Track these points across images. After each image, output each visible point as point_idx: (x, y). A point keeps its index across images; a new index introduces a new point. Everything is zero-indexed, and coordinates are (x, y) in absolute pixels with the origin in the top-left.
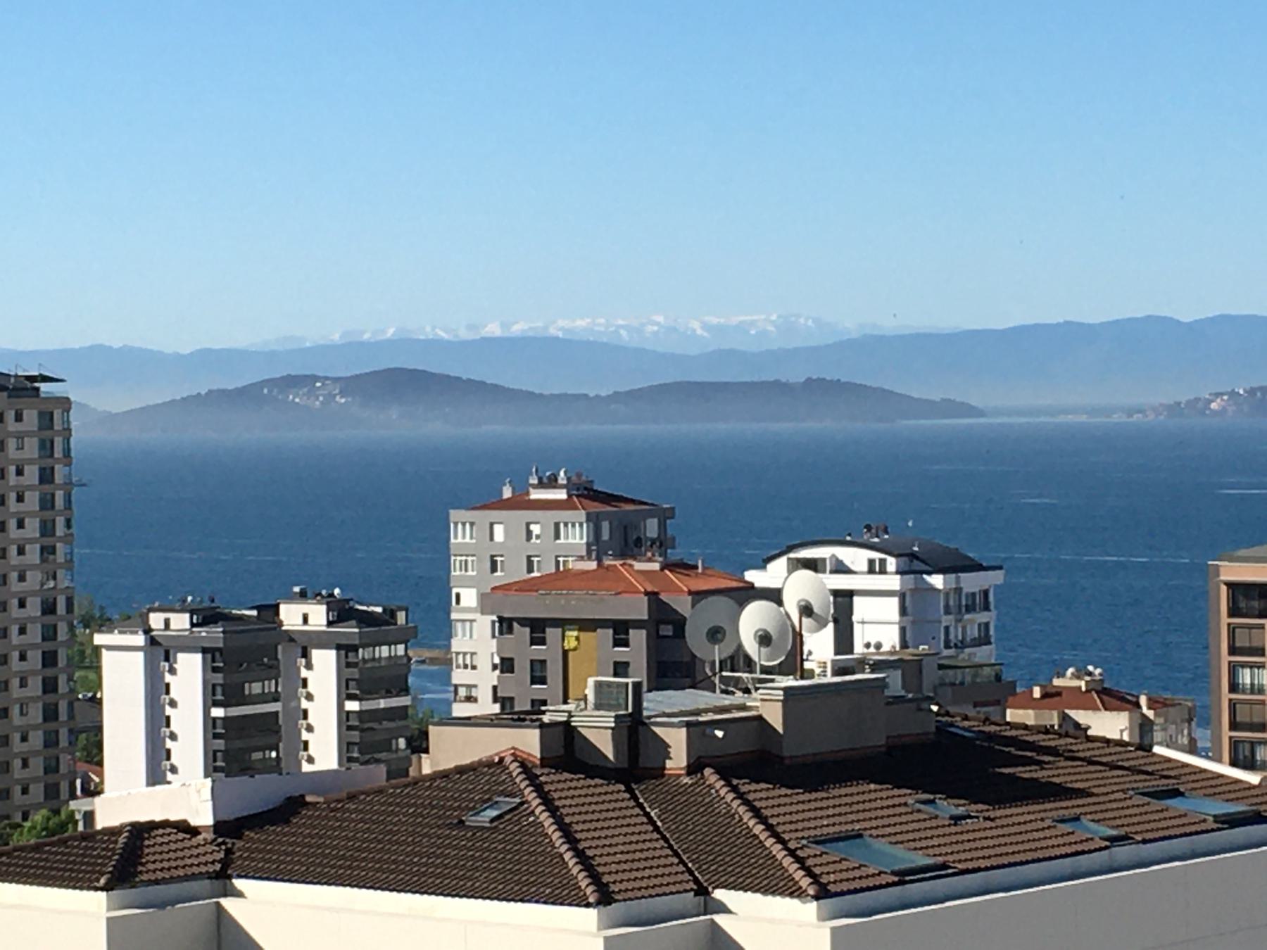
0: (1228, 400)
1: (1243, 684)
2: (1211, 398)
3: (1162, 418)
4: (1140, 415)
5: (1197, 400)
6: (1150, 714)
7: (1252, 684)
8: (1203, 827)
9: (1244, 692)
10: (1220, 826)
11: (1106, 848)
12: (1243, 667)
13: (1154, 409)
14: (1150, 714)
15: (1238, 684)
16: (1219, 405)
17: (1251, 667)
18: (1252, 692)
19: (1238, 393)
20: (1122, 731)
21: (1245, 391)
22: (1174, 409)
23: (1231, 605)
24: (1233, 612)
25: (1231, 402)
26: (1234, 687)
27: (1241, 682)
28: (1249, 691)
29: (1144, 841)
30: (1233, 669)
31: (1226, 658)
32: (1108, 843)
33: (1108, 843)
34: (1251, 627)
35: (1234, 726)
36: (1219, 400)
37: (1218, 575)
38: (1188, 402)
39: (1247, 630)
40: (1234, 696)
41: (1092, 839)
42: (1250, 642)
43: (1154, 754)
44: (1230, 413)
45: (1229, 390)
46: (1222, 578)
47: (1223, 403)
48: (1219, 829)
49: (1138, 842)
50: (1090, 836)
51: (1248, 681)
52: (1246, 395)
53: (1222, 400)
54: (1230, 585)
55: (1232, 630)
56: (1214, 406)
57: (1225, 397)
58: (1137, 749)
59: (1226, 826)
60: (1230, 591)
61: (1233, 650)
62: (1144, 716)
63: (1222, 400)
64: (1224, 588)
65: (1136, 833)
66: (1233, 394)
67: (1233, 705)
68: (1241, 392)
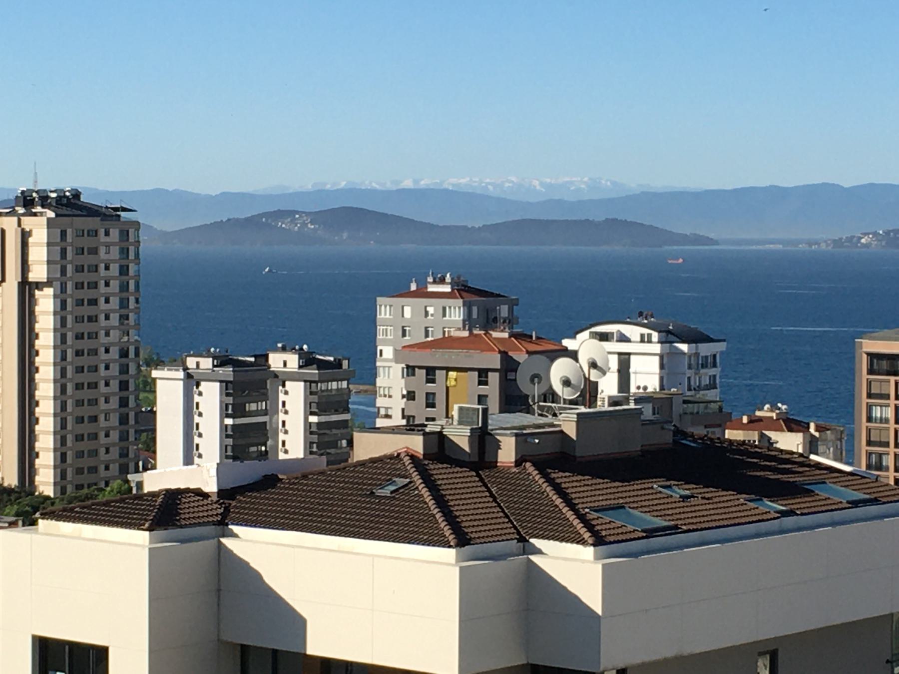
0: (873, 237)
1: (876, 417)
2: (862, 236)
3: (830, 248)
4: (816, 246)
5: (853, 237)
6: (817, 434)
7: (881, 418)
8: (840, 506)
9: (876, 422)
10: (850, 505)
11: (778, 518)
12: (876, 406)
13: (825, 241)
14: (817, 434)
15: (872, 417)
16: (866, 240)
17: (881, 406)
18: (881, 422)
19: (879, 233)
20: (798, 445)
21: (883, 232)
22: (838, 243)
23: (869, 367)
24: (871, 371)
25: (874, 239)
26: (869, 419)
27: (874, 415)
28: (878, 421)
29: (802, 514)
30: (869, 408)
31: (865, 400)
32: (779, 515)
33: (779, 515)
34: (881, 381)
35: (869, 443)
36: (866, 237)
37: (862, 349)
38: (847, 238)
39: (879, 383)
40: (869, 424)
41: (769, 512)
42: (881, 390)
43: (810, 460)
44: (873, 246)
45: (873, 230)
46: (865, 350)
47: (869, 239)
48: (849, 508)
49: (797, 515)
50: (768, 510)
51: (879, 415)
52: (884, 234)
53: (869, 237)
54: (868, 354)
55: (869, 383)
56: (863, 241)
57: (871, 236)
58: (799, 457)
59: (854, 506)
60: (869, 357)
61: (870, 396)
62: (812, 436)
63: (869, 237)
64: (865, 356)
65: (797, 509)
66: (875, 234)
67: (869, 431)
68: (881, 232)
